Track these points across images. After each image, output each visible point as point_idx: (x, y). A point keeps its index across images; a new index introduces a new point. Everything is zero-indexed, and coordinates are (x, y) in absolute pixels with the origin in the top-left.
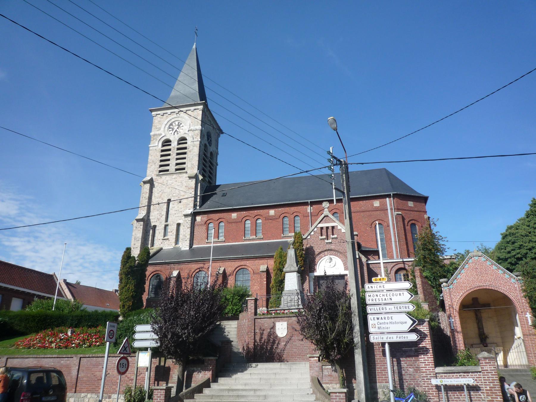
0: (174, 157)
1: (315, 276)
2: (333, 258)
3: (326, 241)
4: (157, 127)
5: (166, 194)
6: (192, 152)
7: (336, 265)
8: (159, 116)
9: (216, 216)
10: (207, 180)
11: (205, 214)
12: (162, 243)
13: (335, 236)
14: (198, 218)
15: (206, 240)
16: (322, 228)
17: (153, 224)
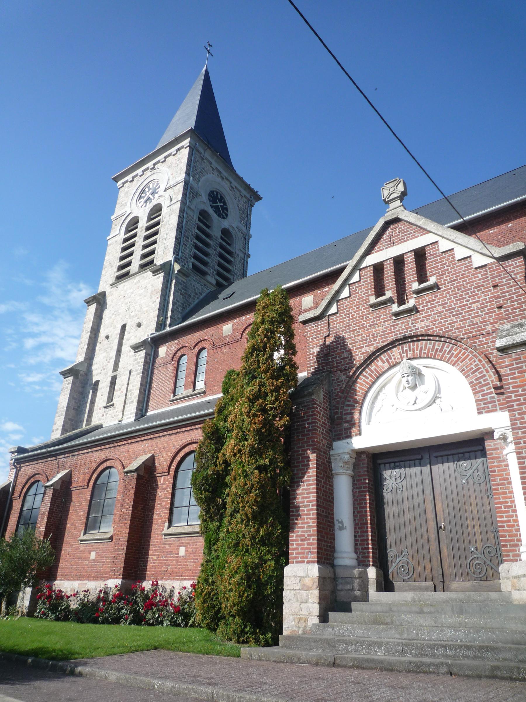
0: (140, 245)
1: (360, 453)
2: (424, 371)
3: (395, 308)
4: (123, 203)
5: (121, 316)
6: (167, 226)
7: (442, 395)
8: (126, 185)
9: (190, 339)
10: (214, 282)
11: (174, 340)
12: (103, 416)
13: (432, 280)
14: (162, 351)
15: (172, 396)
16: (378, 269)
17: (94, 379)
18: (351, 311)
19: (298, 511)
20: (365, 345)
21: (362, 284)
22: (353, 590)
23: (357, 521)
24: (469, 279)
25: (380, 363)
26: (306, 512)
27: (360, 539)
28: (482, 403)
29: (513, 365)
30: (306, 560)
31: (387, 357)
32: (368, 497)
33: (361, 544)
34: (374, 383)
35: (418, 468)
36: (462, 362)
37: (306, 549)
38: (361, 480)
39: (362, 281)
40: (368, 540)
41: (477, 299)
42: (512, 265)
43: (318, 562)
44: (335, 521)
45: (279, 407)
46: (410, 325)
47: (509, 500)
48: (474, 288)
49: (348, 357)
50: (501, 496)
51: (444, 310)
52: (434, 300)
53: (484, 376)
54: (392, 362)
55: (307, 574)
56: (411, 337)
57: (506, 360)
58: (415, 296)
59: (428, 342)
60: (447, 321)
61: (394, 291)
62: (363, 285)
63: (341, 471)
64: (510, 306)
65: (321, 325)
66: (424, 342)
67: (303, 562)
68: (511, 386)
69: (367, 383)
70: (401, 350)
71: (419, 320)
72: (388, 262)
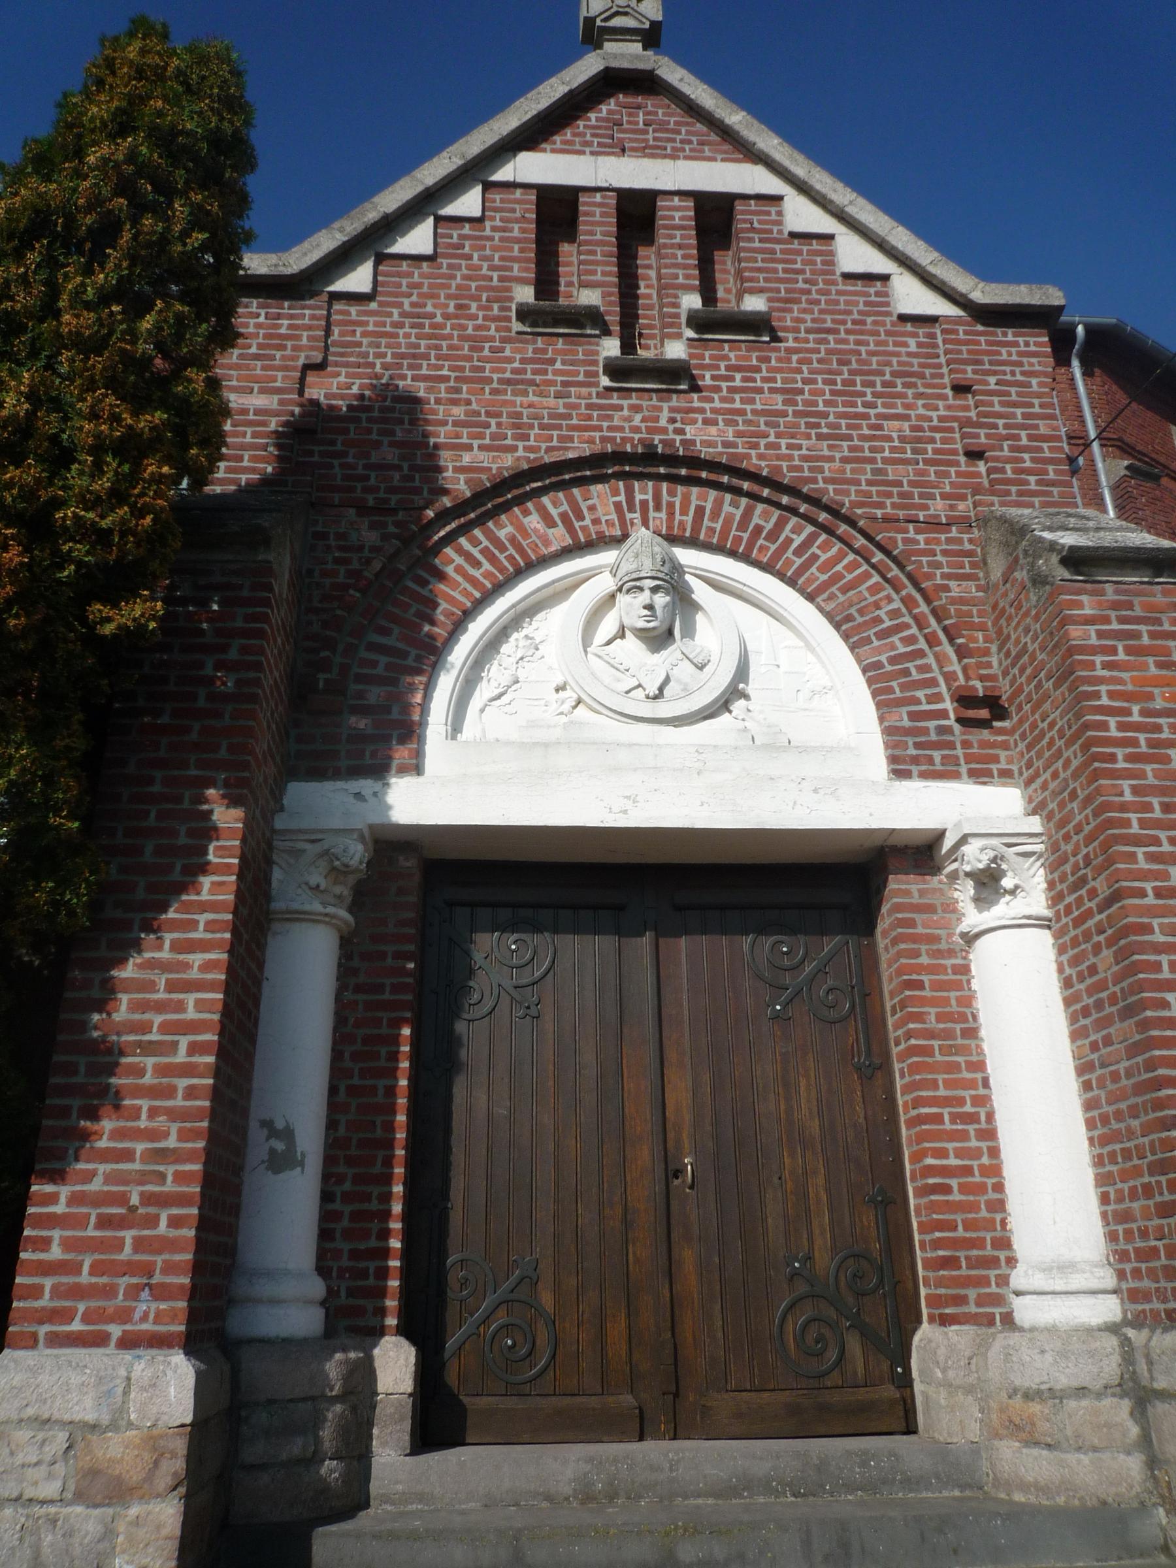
2: (701, 592)
7: (750, 689)
18: (429, 308)
19: (111, 1069)
20: (476, 443)
21: (488, 232)
22: (316, 1459)
23: (342, 1131)
24: (877, 344)
25: (533, 521)
26: (148, 1079)
27: (347, 1209)
28: (910, 741)
29: (1106, 620)
30: (116, 1331)
31: (565, 507)
32: (406, 1031)
33: (348, 1235)
34: (499, 588)
35: (604, 944)
36: (845, 590)
37: (129, 1268)
38: (383, 955)
39: (488, 224)
40: (387, 1215)
41: (900, 410)
42: (1016, 344)
43: (191, 1345)
44: (253, 1125)
45: (123, 535)
46: (663, 422)
47: (967, 1094)
48: (894, 374)
49: (399, 468)
50: (940, 1077)
51: (790, 410)
52: (758, 370)
53: (920, 654)
54: (583, 528)
55: (122, 1410)
56: (672, 460)
57: (1085, 598)
58: (690, 333)
59: (728, 497)
60: (800, 447)
61: (610, 294)
62: (491, 239)
63: (317, 907)
64: (1008, 460)
65: (292, 317)
66: (713, 494)
67: (98, 1340)
68: (1103, 688)
69: (473, 581)
70: (622, 498)
71: (700, 417)
72: (598, 197)
